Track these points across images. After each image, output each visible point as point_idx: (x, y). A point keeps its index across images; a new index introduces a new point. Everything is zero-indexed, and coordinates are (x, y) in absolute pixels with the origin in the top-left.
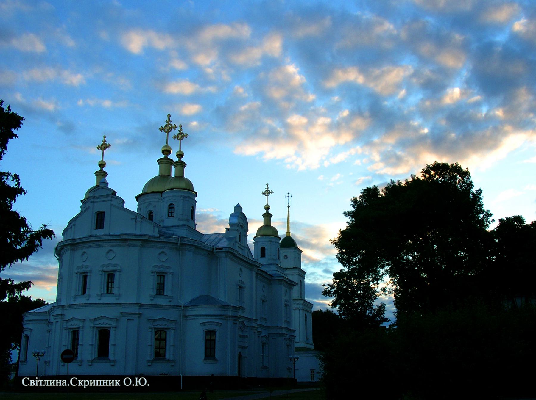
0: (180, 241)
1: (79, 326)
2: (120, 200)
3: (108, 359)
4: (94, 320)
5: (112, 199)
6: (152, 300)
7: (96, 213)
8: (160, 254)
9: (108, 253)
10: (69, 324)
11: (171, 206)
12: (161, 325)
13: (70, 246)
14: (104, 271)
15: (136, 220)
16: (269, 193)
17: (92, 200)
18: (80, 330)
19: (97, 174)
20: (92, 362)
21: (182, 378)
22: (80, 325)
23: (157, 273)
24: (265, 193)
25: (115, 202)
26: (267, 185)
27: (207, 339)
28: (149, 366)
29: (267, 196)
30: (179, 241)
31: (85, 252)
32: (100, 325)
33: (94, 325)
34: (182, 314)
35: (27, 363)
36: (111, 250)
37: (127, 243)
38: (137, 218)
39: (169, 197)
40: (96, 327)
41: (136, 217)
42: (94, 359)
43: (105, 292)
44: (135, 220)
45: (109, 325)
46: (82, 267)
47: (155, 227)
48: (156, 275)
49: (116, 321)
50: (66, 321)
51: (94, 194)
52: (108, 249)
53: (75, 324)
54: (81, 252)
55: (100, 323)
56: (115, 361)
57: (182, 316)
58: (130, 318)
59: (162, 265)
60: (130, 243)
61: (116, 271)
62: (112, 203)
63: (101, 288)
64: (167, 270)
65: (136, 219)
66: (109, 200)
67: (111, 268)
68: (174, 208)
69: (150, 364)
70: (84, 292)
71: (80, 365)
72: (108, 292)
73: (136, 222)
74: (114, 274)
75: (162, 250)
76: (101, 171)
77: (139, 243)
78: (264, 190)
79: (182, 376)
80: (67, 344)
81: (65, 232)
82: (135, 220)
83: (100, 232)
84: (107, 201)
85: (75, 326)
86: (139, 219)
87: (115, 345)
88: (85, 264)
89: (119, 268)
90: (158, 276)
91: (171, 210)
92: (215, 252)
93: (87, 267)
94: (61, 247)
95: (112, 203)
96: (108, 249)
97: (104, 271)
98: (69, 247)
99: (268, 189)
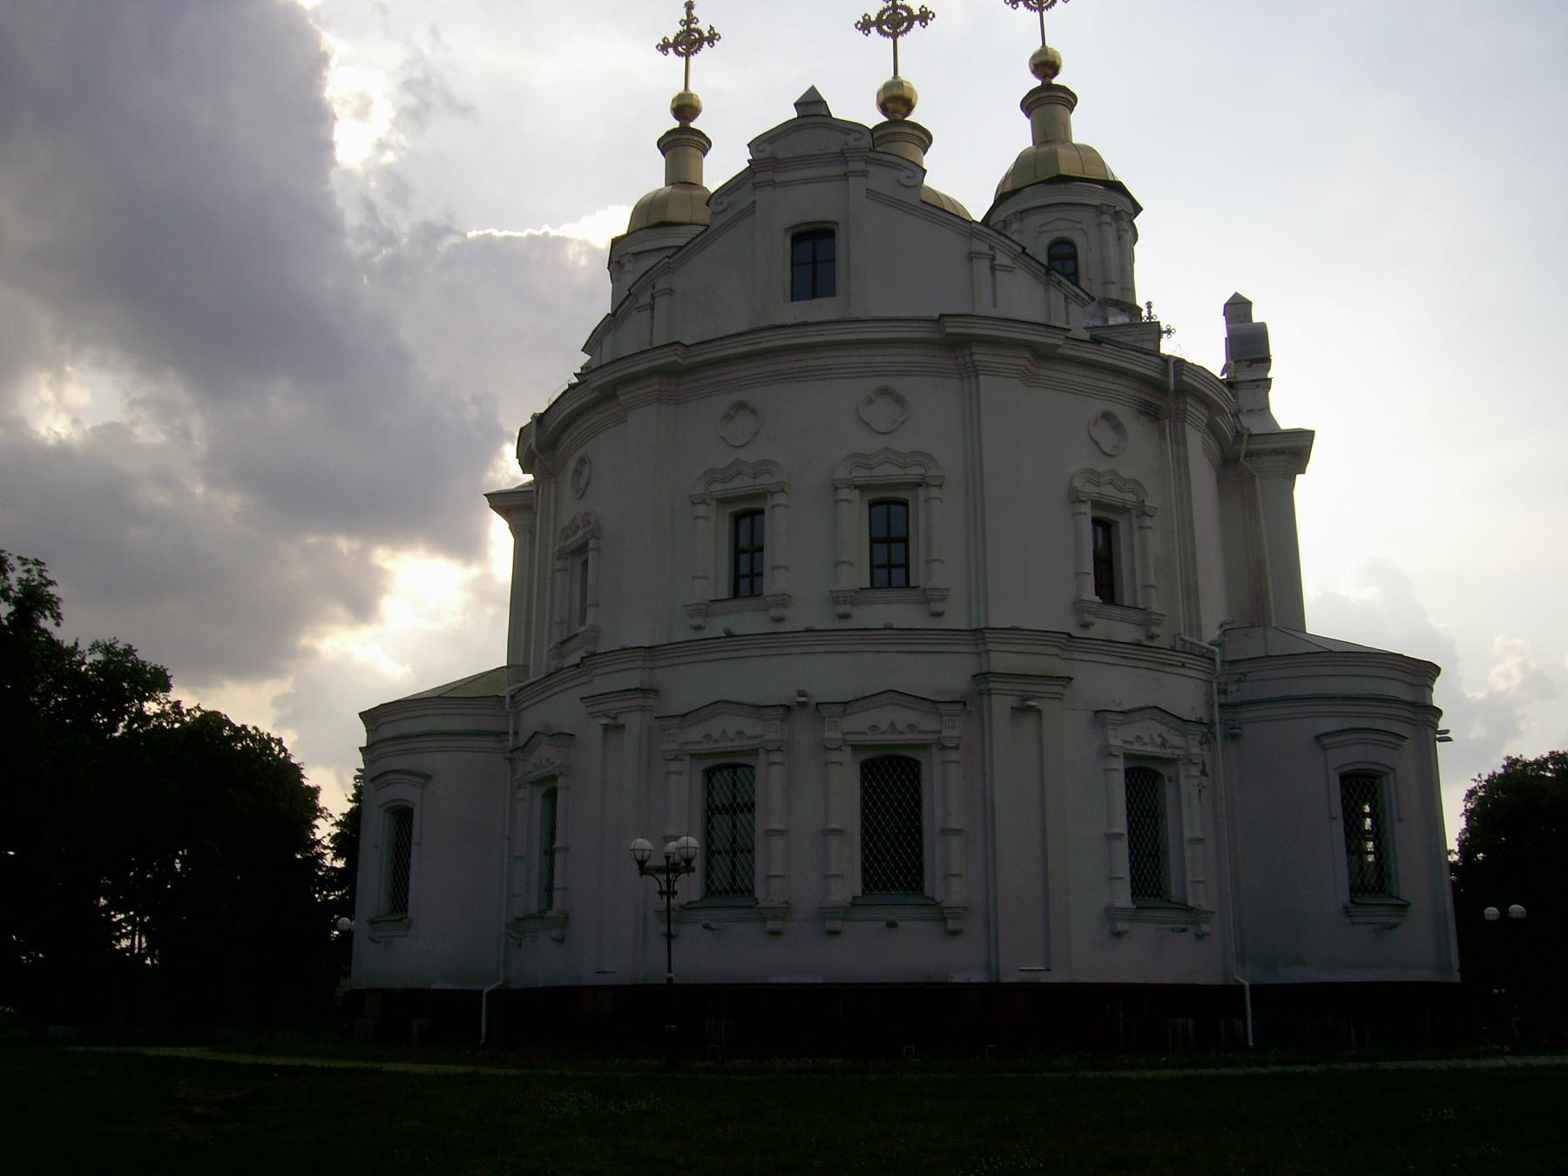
2: (911, 174)
5: (872, 169)
7: (786, 230)
15: (995, 263)
21: (1248, 993)
23: (1096, 504)
32: (872, 738)
33: (843, 734)
35: (409, 927)
38: (997, 251)
41: (991, 248)
44: (987, 262)
50: (676, 721)
57: (1216, 705)
60: (982, 356)
65: (993, 258)
66: (856, 174)
68: (1074, 257)
73: (993, 269)
74: (905, 504)
79: (1247, 984)
82: (988, 261)
83: (821, 309)
88: (749, 456)
92: (1243, 454)
94: (596, 394)
98: (656, 387)
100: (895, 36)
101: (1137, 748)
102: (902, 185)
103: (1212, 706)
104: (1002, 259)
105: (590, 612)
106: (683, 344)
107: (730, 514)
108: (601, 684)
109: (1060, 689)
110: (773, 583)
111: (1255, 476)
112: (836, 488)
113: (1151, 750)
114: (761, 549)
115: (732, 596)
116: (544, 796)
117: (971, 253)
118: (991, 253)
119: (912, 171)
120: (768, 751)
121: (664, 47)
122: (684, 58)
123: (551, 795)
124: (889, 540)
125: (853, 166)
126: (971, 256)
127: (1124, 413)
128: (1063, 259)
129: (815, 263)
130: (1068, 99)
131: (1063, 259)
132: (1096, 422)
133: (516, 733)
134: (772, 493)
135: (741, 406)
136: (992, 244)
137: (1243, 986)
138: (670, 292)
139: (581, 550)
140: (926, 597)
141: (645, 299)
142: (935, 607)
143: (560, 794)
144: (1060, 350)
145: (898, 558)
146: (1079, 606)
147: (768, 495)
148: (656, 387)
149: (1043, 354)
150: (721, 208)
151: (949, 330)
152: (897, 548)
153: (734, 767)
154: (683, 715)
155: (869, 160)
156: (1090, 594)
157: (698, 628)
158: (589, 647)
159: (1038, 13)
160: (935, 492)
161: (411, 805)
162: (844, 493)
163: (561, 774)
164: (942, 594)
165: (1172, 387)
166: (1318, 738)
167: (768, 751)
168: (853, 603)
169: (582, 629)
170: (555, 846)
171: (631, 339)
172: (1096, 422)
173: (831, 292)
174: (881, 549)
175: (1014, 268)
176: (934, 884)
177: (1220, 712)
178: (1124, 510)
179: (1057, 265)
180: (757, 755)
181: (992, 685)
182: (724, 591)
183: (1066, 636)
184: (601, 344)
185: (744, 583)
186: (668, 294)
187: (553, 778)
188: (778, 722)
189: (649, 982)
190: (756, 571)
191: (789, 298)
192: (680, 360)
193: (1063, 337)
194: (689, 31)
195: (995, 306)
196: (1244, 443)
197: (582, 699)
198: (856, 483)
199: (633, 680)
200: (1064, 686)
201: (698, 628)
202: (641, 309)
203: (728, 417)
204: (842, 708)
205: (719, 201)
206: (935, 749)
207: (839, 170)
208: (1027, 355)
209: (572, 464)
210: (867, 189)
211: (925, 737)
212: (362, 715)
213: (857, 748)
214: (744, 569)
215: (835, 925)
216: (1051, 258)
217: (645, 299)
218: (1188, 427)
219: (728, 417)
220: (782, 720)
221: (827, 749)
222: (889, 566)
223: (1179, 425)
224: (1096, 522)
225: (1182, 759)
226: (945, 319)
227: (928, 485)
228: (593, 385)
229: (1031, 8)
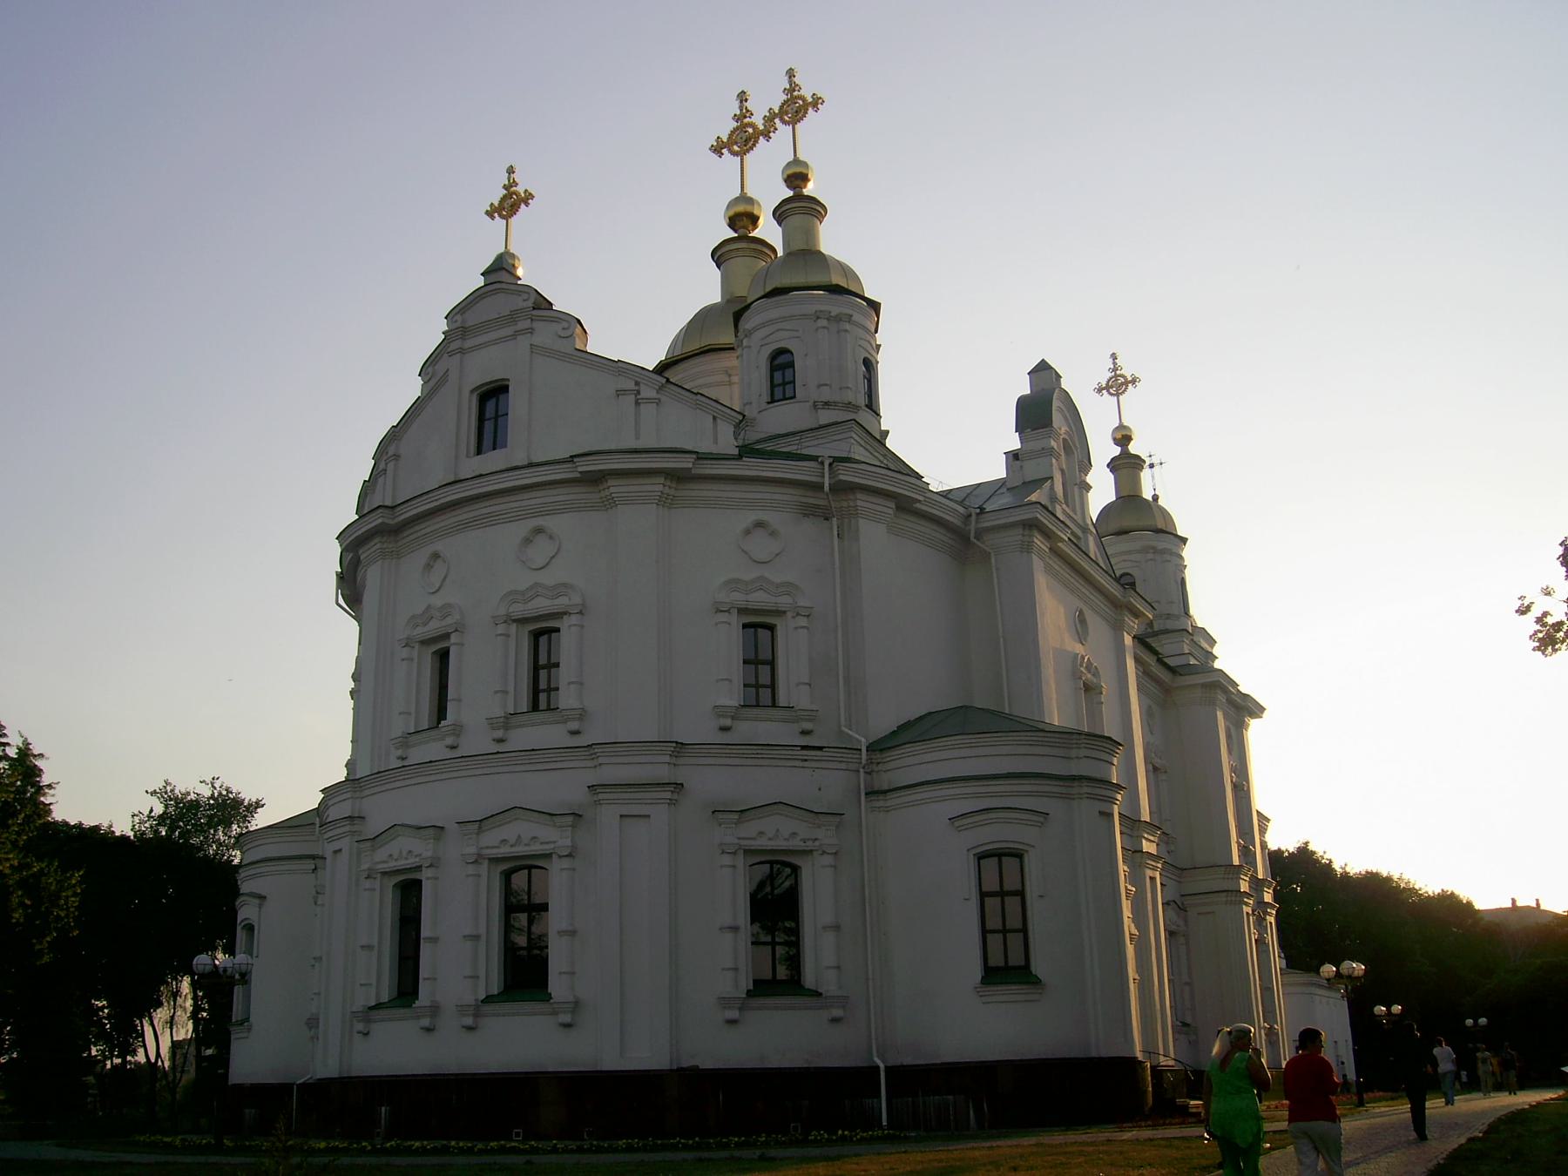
1: (417, 860)
3: (548, 998)
4: (480, 827)
5: (535, 325)
6: (724, 729)
7: (472, 391)
8: (747, 532)
9: (527, 541)
10: (381, 854)
12: (777, 833)
14: (514, 621)
15: (638, 397)
16: (1122, 384)
18: (425, 875)
20: (476, 1016)
22: (424, 856)
23: (742, 611)
24: (1108, 388)
25: (545, 335)
26: (1114, 356)
27: (984, 889)
29: (1118, 395)
30: (827, 475)
31: (436, 556)
32: (505, 851)
34: (862, 786)
36: (539, 531)
39: (763, 325)
40: (490, 859)
41: (637, 384)
42: (489, 999)
43: (524, 706)
45: (542, 843)
46: (427, 615)
47: (719, 421)
48: (736, 621)
49: (573, 826)
51: (463, 321)
52: (523, 528)
53: (404, 854)
54: (423, 555)
55: (504, 841)
56: (576, 1005)
58: (635, 810)
59: (762, 578)
60: (616, 487)
61: (565, 613)
62: (537, 339)
63: (505, 692)
65: (639, 392)
67: (542, 605)
68: (791, 365)
69: (734, 1014)
70: (441, 713)
72: (535, 707)
73: (637, 403)
75: (752, 517)
77: (656, 486)
78: (1104, 377)
79: (882, 1066)
81: (366, 494)
83: (493, 460)
84: (514, 336)
86: (648, 392)
87: (572, 933)
89: (577, 600)
90: (745, 626)
91: (778, 375)
93: (446, 610)
95: (537, 339)
96: (523, 528)
97: (514, 621)
98: (378, 546)
99: (1118, 372)
102: (560, 337)
118: (637, 388)
126: (620, 393)
130: (815, 209)
136: (639, 380)
137: (878, 1068)
142: (574, 726)
148: (378, 546)
162: (501, 629)
165: (827, 488)
177: (866, 802)
181: (601, 796)
183: (674, 745)
188: (432, 841)
189: (353, 1074)
193: (693, 460)
195: (637, 438)
196: (973, 523)
204: (476, 826)
208: (662, 480)
210: (531, 345)
211: (546, 847)
218: (861, 520)
223: (853, 521)
225: (817, 850)
226: (575, 460)
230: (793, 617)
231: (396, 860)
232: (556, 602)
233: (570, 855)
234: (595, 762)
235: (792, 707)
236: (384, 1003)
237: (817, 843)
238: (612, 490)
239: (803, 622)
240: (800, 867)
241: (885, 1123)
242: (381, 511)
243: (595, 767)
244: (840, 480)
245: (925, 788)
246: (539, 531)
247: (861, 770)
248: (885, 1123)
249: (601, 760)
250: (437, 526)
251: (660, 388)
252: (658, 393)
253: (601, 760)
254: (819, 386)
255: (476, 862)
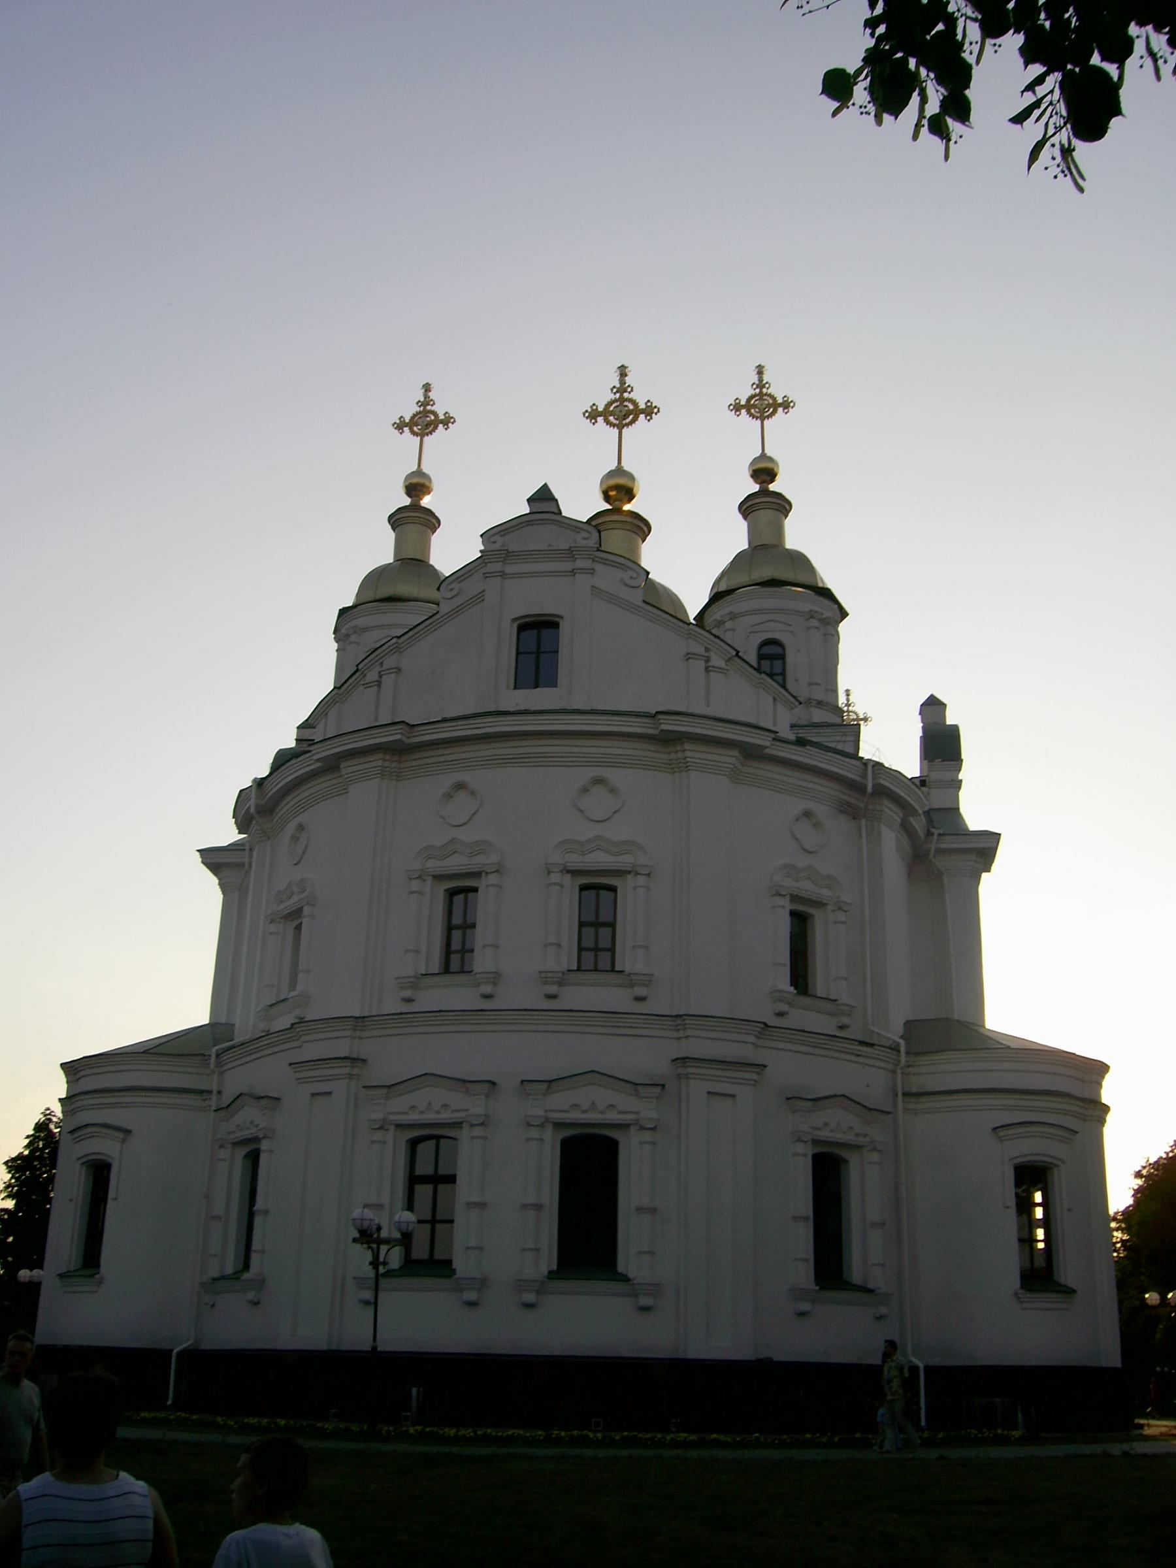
0: (873, 775)
2: (635, 575)
4: (549, 1086)
5: (599, 567)
7: (514, 620)
11: (768, 650)
13: (380, 756)
14: (569, 872)
15: (710, 664)
17: (497, 567)
19: (397, 520)
23: (795, 898)
28: (802, 1314)
35: (101, 1283)
37: (680, 755)
39: (755, 612)
41: (707, 650)
50: (384, 1091)
57: (900, 1095)
60: (693, 752)
61: (629, 872)
64: (826, 892)
65: (708, 660)
66: (582, 570)
67: (600, 859)
68: (782, 657)
69: (805, 1306)
71: (472, 1304)
73: (707, 670)
74: (613, 889)
76: (415, 507)
77: (730, 758)
79: (921, 1366)
80: (386, 1200)
84: (573, 573)
85: (430, 1117)
86: (717, 661)
92: (933, 850)
94: (319, 764)
97: (569, 872)
100: (620, 427)
101: (825, 1134)
102: (627, 585)
103: (897, 1095)
104: (717, 661)
105: (301, 977)
106: (407, 724)
107: (445, 890)
108: (310, 1051)
109: (754, 1076)
110: (482, 962)
111: (943, 874)
112: (549, 872)
113: (840, 1137)
114: (473, 926)
115: (442, 971)
116: (246, 1156)
117: (689, 654)
119: (636, 572)
120: (472, 1125)
121: (400, 426)
122: (419, 438)
123: (254, 1158)
124: (597, 924)
125: (580, 563)
126: (689, 656)
127: (822, 811)
128: (771, 657)
129: (538, 653)
130: (782, 506)
131: (771, 657)
132: (797, 820)
133: (219, 1092)
134: (487, 873)
135: (460, 786)
136: (708, 646)
138: (398, 670)
139: (296, 914)
140: (630, 981)
141: (372, 676)
142: (641, 991)
143: (263, 1158)
144: (767, 751)
145: (604, 942)
146: (777, 995)
147: (483, 875)
148: (380, 763)
149: (751, 753)
150: (449, 595)
151: (664, 727)
152: (605, 932)
153: (438, 1138)
154: (390, 1087)
155: (596, 559)
156: (785, 984)
157: (409, 1000)
158: (297, 1012)
159: (759, 422)
160: (641, 880)
161: (111, 1161)
162: (555, 878)
163: (265, 1137)
164: (648, 980)
165: (870, 789)
166: (995, 1129)
167: (472, 1125)
168: (561, 983)
169: (292, 994)
170: (255, 1208)
171: (358, 713)
172: (797, 820)
173: (553, 683)
174: (589, 932)
175: (728, 670)
176: (628, 1260)
177: (903, 1102)
178: (820, 904)
179: (766, 664)
180: (461, 1128)
181: (690, 1070)
182: (435, 967)
183: (762, 1025)
184: (326, 714)
185: (455, 959)
186: (396, 672)
187: (256, 1139)
188: (483, 1097)
189: (343, 1348)
190: (467, 947)
191: (512, 685)
192: (404, 739)
193: (771, 739)
194: (426, 413)
195: (708, 705)
196: (934, 841)
197: (291, 1064)
198: (568, 868)
199: (343, 1048)
200: (758, 1074)
201: (409, 1000)
202: (367, 685)
203: (448, 796)
204: (545, 1086)
205: (450, 587)
206: (633, 1129)
207: (568, 566)
209: (291, 828)
210: (592, 586)
212: (65, 1066)
213: (558, 1125)
214: (456, 945)
215: (530, 1297)
216: (761, 657)
217: (372, 676)
218: (882, 826)
219: (448, 796)
220: (487, 1096)
221: (529, 1125)
222: (597, 950)
224: (793, 914)
227: (637, 874)
228: (315, 757)
229: (753, 416)
230: (833, 911)
231: (422, 1112)
232: (621, 859)
233: (483, 1124)
234: (681, 1034)
235: (836, 1000)
236: (394, 1270)
237: (866, 1139)
238: (688, 754)
239: (841, 916)
240: (847, 1161)
241: (923, 1423)
242: (400, 727)
243: (679, 1039)
244: (880, 784)
245: (962, 1096)
246: (599, 781)
247: (899, 1071)
248: (923, 1423)
249: (689, 1032)
250: (467, 755)
251: (730, 658)
252: (726, 664)
253: (689, 1032)
254: (810, 684)
255: (541, 1126)
